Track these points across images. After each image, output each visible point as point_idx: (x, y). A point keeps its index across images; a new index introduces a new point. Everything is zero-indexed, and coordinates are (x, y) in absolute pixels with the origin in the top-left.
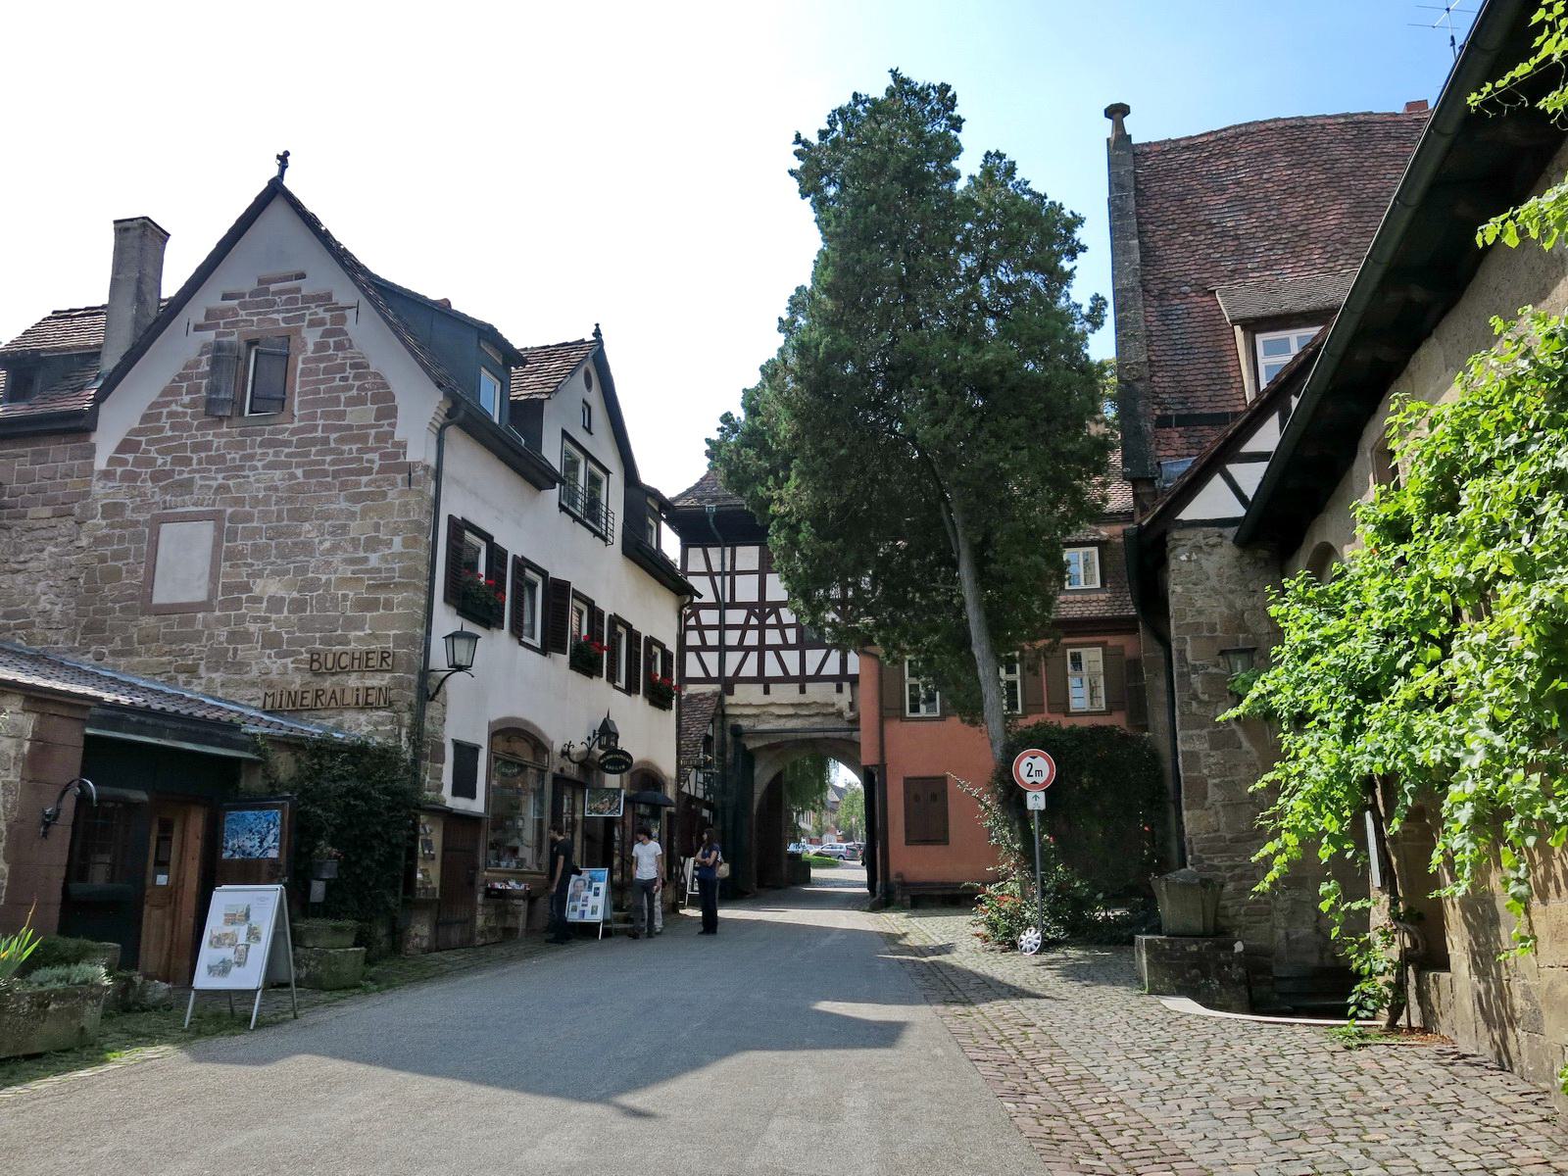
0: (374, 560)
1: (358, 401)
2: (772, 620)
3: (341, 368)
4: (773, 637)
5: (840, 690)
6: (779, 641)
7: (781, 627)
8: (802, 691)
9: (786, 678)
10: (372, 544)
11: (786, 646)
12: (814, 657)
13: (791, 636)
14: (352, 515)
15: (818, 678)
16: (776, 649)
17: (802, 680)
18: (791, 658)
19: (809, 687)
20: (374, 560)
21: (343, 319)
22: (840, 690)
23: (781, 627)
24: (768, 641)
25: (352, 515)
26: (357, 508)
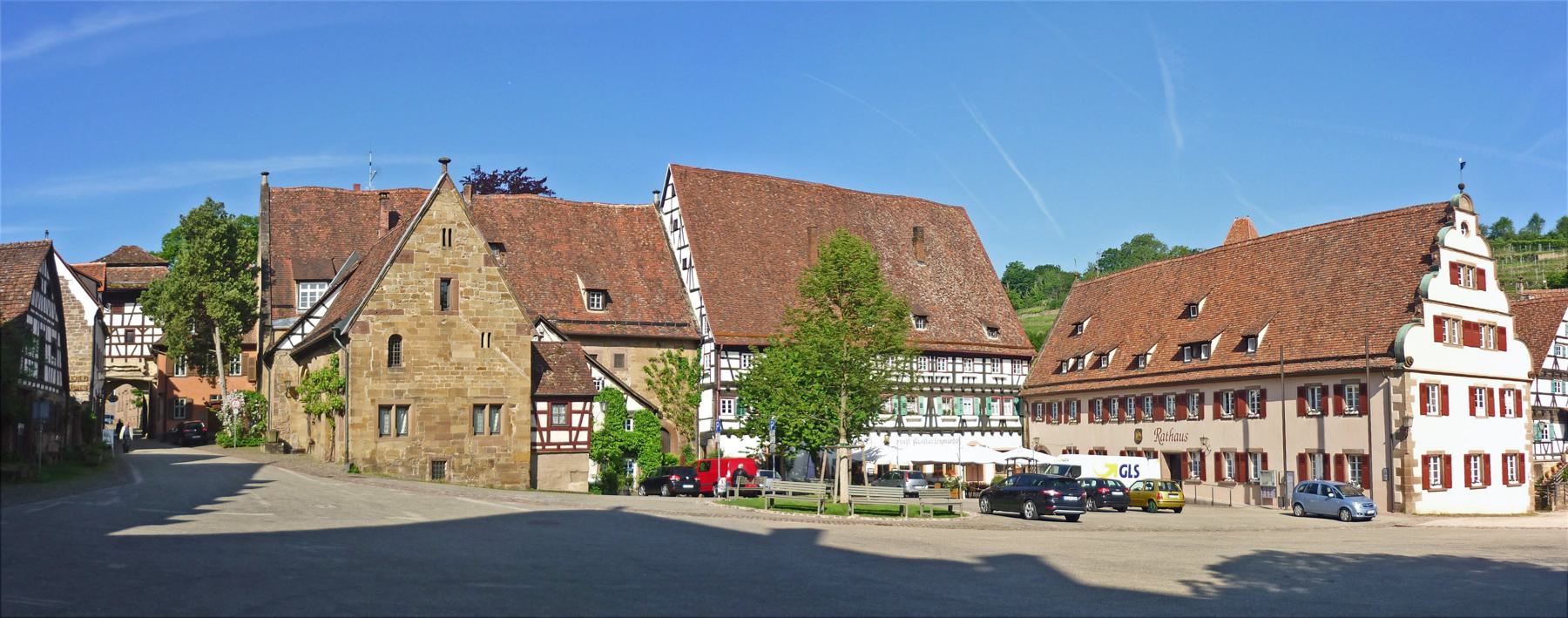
0: (81, 352)
1: (74, 308)
2: (115, 333)
3: (68, 298)
4: (115, 340)
5: (140, 361)
6: (117, 342)
7: (118, 336)
8: (126, 361)
9: (120, 357)
10: (80, 348)
11: (120, 344)
12: (131, 348)
13: (122, 340)
14: (74, 340)
15: (132, 356)
16: (116, 344)
17: (126, 357)
18: (122, 349)
19: (129, 359)
20: (81, 352)
21: (67, 284)
22: (140, 361)
23: (118, 336)
24: (113, 342)
25: (74, 340)
26: (75, 338)
